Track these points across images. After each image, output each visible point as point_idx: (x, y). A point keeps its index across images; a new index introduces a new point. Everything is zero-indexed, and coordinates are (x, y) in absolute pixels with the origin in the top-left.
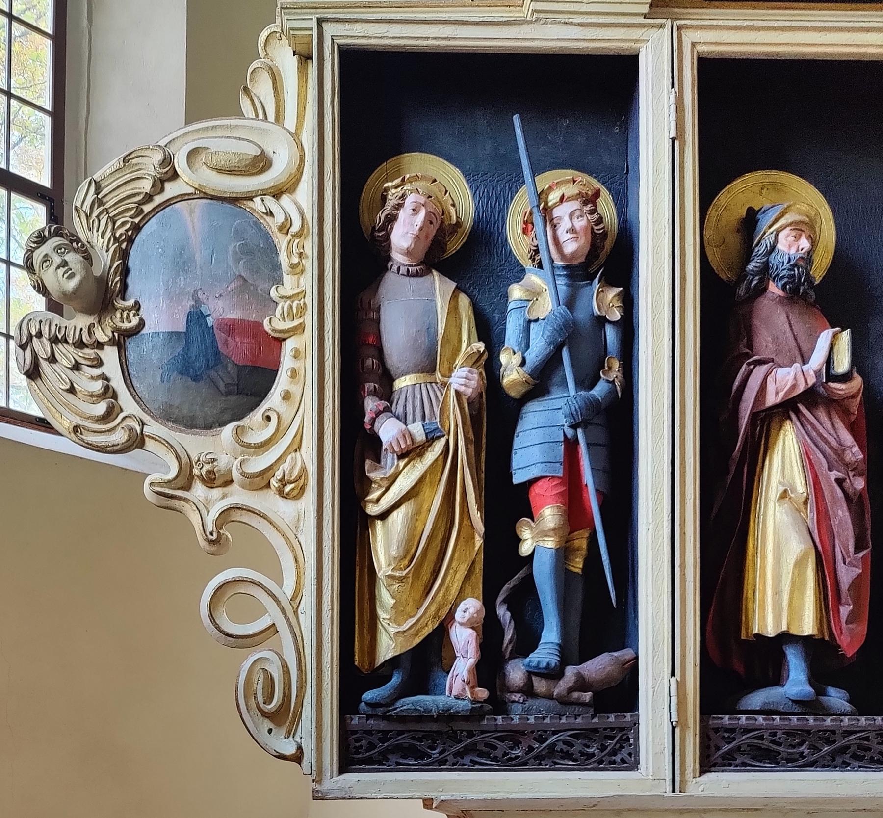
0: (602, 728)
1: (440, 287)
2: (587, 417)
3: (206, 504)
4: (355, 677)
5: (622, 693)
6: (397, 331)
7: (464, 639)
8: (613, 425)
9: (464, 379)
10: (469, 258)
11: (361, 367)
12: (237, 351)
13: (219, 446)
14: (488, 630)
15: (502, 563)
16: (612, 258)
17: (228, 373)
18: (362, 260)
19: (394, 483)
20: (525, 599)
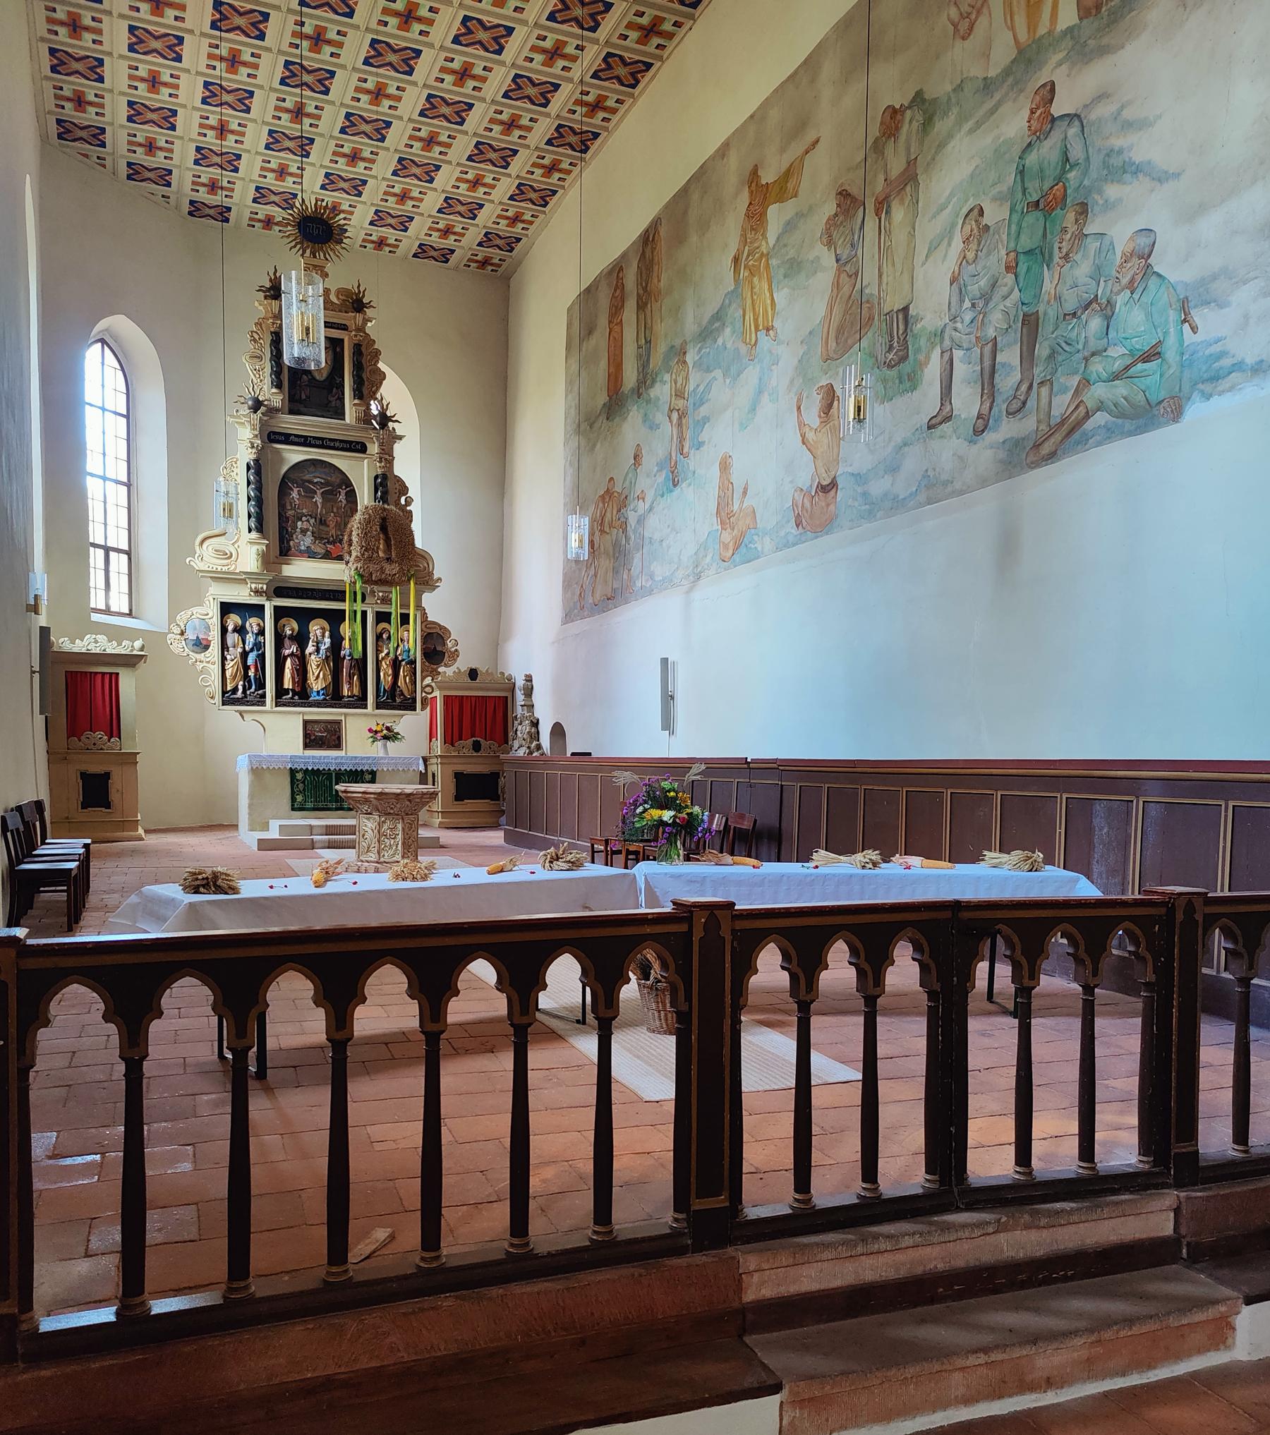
0: (261, 700)
1: (236, 635)
2: (258, 656)
3: (200, 666)
4: (224, 692)
5: (263, 696)
6: (229, 642)
7: (240, 688)
8: (262, 657)
9: (240, 650)
10: (241, 630)
11: (224, 647)
12: (204, 643)
13: (201, 656)
14: (244, 686)
15: (246, 676)
16: (261, 632)
17: (202, 645)
19: (229, 664)
20: (250, 682)
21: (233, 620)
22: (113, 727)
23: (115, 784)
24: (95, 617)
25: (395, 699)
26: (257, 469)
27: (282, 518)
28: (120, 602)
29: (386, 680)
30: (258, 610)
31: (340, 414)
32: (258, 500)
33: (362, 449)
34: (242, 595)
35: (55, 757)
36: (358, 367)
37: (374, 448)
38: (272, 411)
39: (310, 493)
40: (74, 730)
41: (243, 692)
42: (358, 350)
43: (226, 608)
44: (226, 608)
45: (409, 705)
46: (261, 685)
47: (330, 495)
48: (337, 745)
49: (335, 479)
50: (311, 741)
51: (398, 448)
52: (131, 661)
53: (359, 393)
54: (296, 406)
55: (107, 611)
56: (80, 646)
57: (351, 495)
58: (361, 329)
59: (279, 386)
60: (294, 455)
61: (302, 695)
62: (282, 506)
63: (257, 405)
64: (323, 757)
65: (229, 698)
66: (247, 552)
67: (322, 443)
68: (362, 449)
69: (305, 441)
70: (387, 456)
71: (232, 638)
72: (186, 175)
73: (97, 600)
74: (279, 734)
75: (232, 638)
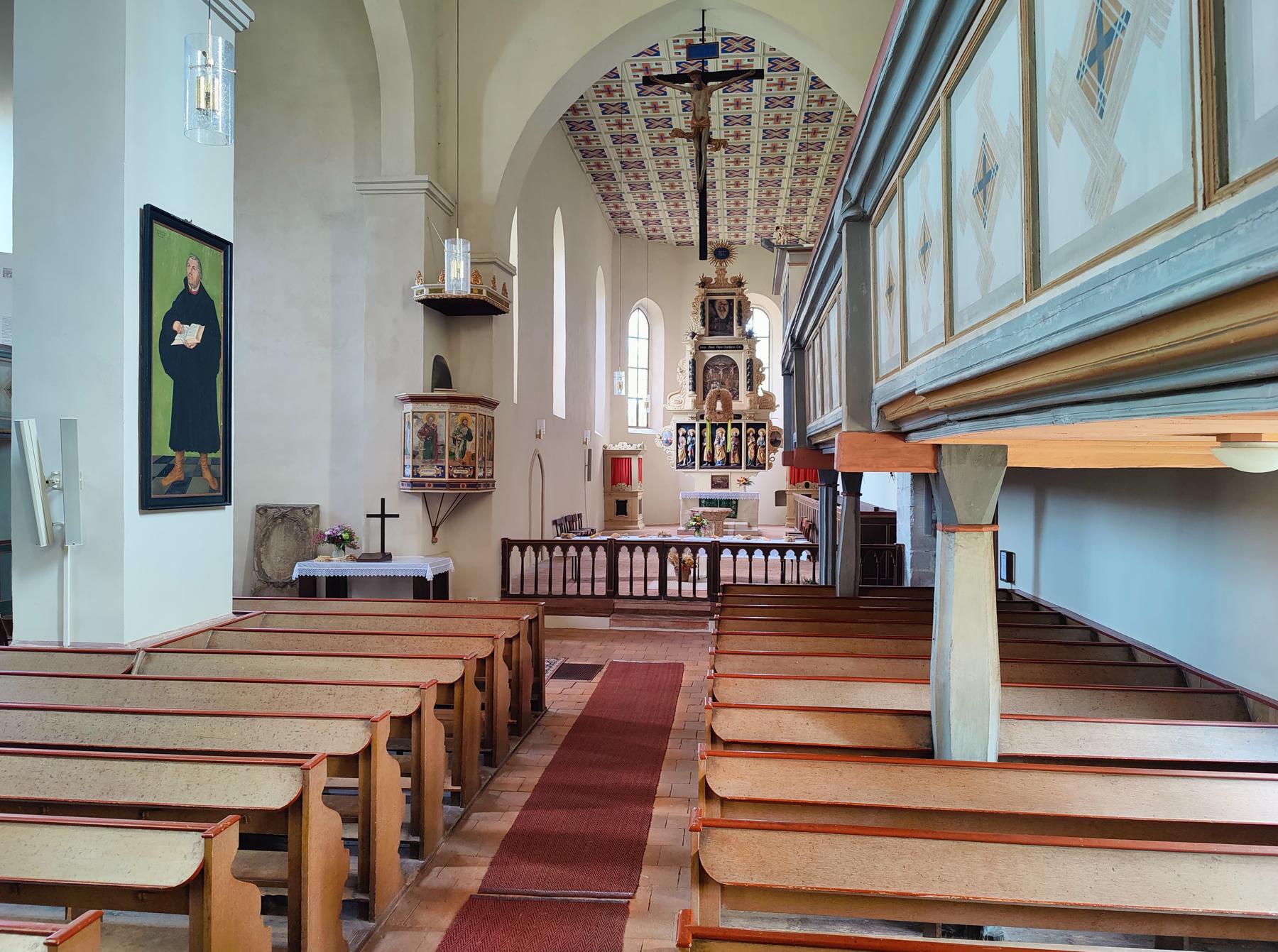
11: (678, 443)
17: (669, 443)
18: (678, 436)
21: (682, 431)
22: (629, 482)
23: (629, 505)
24: (630, 430)
25: (756, 465)
26: (693, 363)
27: (705, 383)
28: (643, 423)
29: (751, 456)
30: (693, 426)
31: (731, 333)
32: (694, 377)
33: (741, 347)
34: (686, 419)
35: (607, 494)
36: (740, 311)
37: (746, 347)
38: (701, 336)
39: (717, 370)
40: (614, 482)
41: (686, 463)
42: (740, 304)
43: (679, 426)
44: (679, 426)
45: (762, 467)
46: (693, 460)
47: (726, 370)
48: (727, 487)
49: (729, 363)
50: (715, 485)
51: (758, 346)
52: (636, 453)
53: (740, 323)
54: (712, 332)
55: (637, 426)
56: (616, 448)
57: (736, 369)
58: (742, 294)
59: (704, 325)
60: (710, 354)
61: (712, 463)
62: (704, 378)
63: (694, 335)
64: (720, 493)
65: (679, 466)
66: (688, 400)
67: (723, 348)
68: (741, 347)
69: (715, 348)
70: (752, 349)
71: (682, 439)
72: (671, 236)
73: (632, 422)
74: (700, 482)
75: (682, 439)
